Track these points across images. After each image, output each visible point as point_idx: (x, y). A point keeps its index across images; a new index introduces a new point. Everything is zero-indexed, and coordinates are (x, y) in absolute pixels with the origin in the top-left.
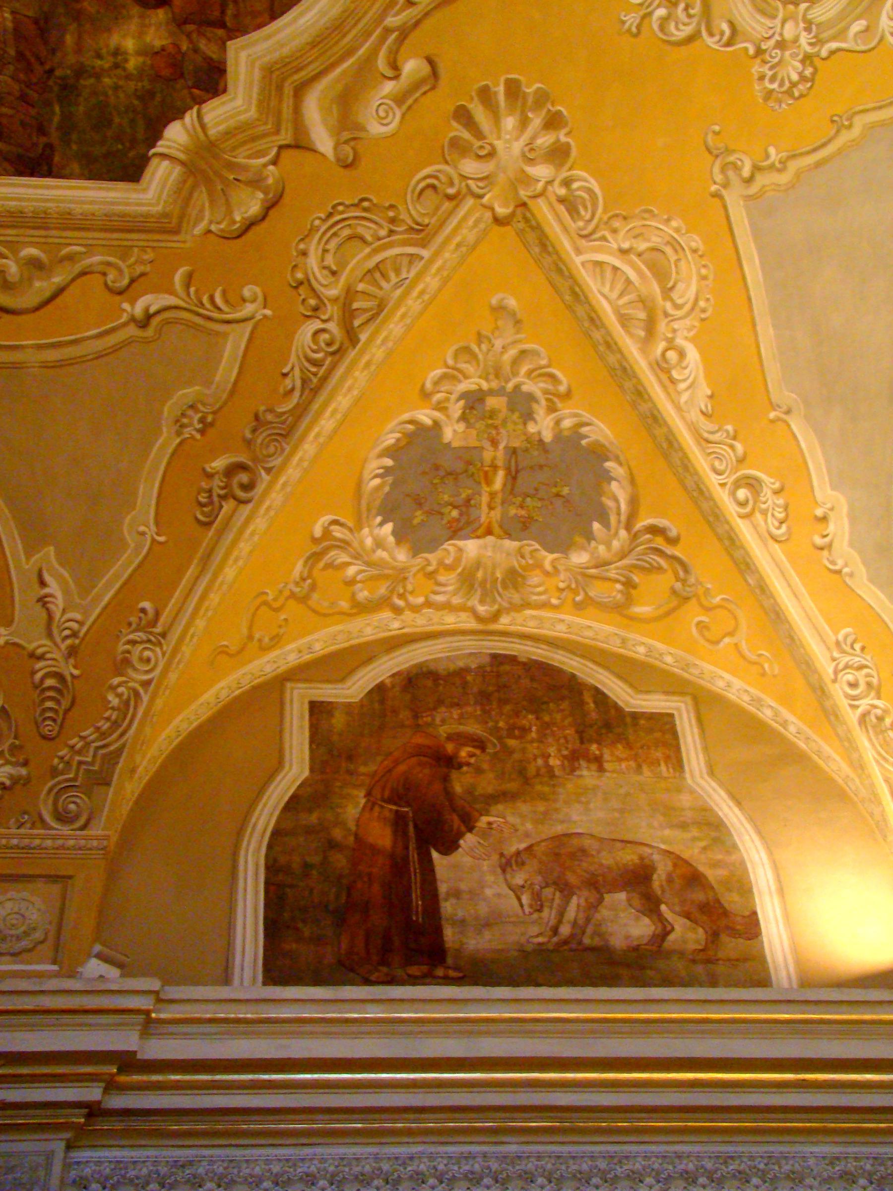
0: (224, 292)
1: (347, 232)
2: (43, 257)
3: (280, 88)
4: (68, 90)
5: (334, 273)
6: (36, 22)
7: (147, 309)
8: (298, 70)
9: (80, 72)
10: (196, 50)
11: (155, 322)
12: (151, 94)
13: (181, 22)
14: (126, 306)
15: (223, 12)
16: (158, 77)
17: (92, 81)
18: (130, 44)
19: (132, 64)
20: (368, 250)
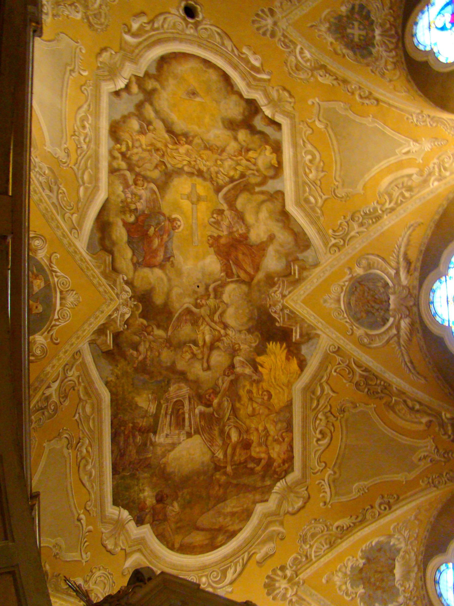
0: (88, 545)
1: (106, 581)
2: (92, 477)
3: (140, 544)
4: (133, 476)
5: (95, 582)
6: (149, 464)
7: (82, 519)
8: (145, 549)
9: (138, 479)
10: (147, 514)
11: (79, 523)
12: (134, 503)
13: (153, 508)
14: (82, 511)
15: (157, 520)
16: (139, 504)
17: (136, 483)
18: (146, 493)
19: (141, 495)
20: (102, 591)
